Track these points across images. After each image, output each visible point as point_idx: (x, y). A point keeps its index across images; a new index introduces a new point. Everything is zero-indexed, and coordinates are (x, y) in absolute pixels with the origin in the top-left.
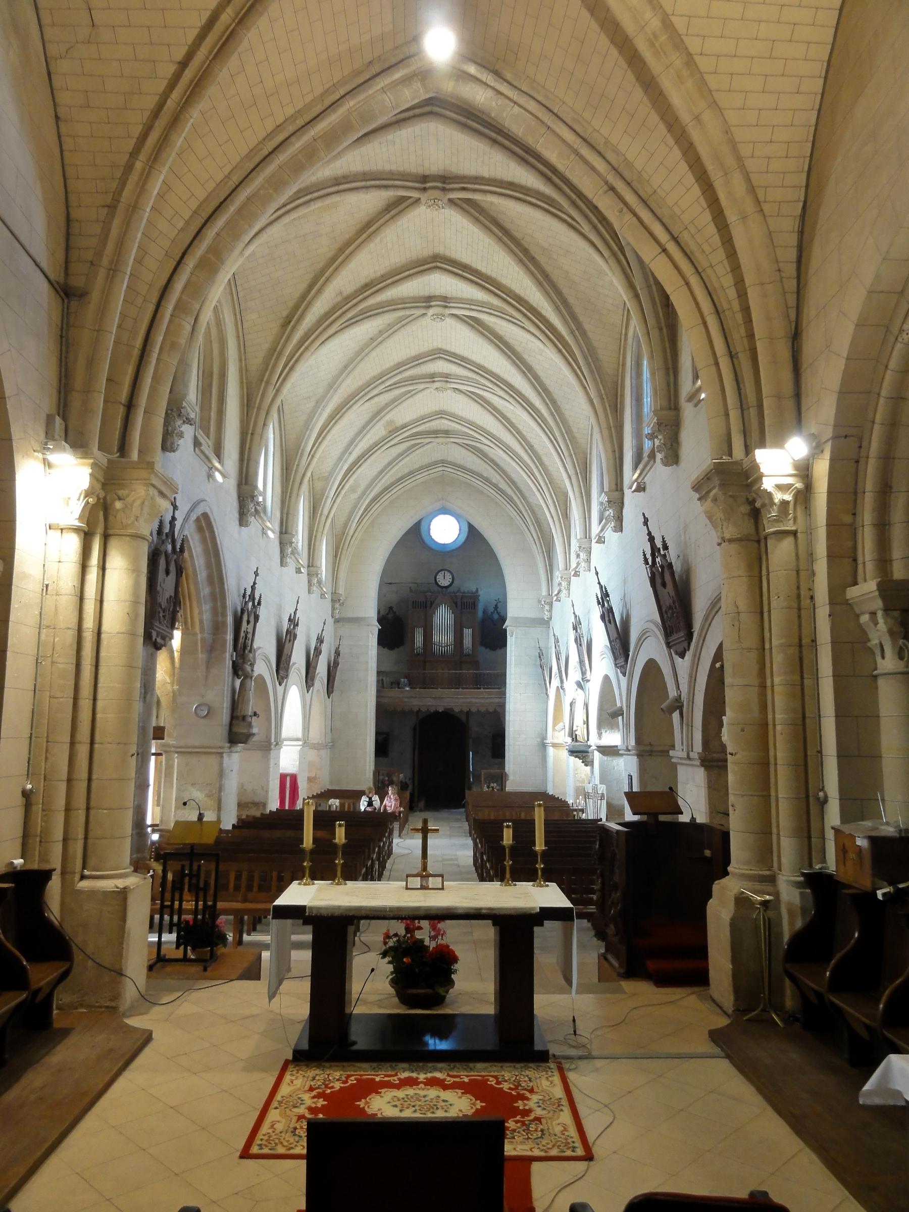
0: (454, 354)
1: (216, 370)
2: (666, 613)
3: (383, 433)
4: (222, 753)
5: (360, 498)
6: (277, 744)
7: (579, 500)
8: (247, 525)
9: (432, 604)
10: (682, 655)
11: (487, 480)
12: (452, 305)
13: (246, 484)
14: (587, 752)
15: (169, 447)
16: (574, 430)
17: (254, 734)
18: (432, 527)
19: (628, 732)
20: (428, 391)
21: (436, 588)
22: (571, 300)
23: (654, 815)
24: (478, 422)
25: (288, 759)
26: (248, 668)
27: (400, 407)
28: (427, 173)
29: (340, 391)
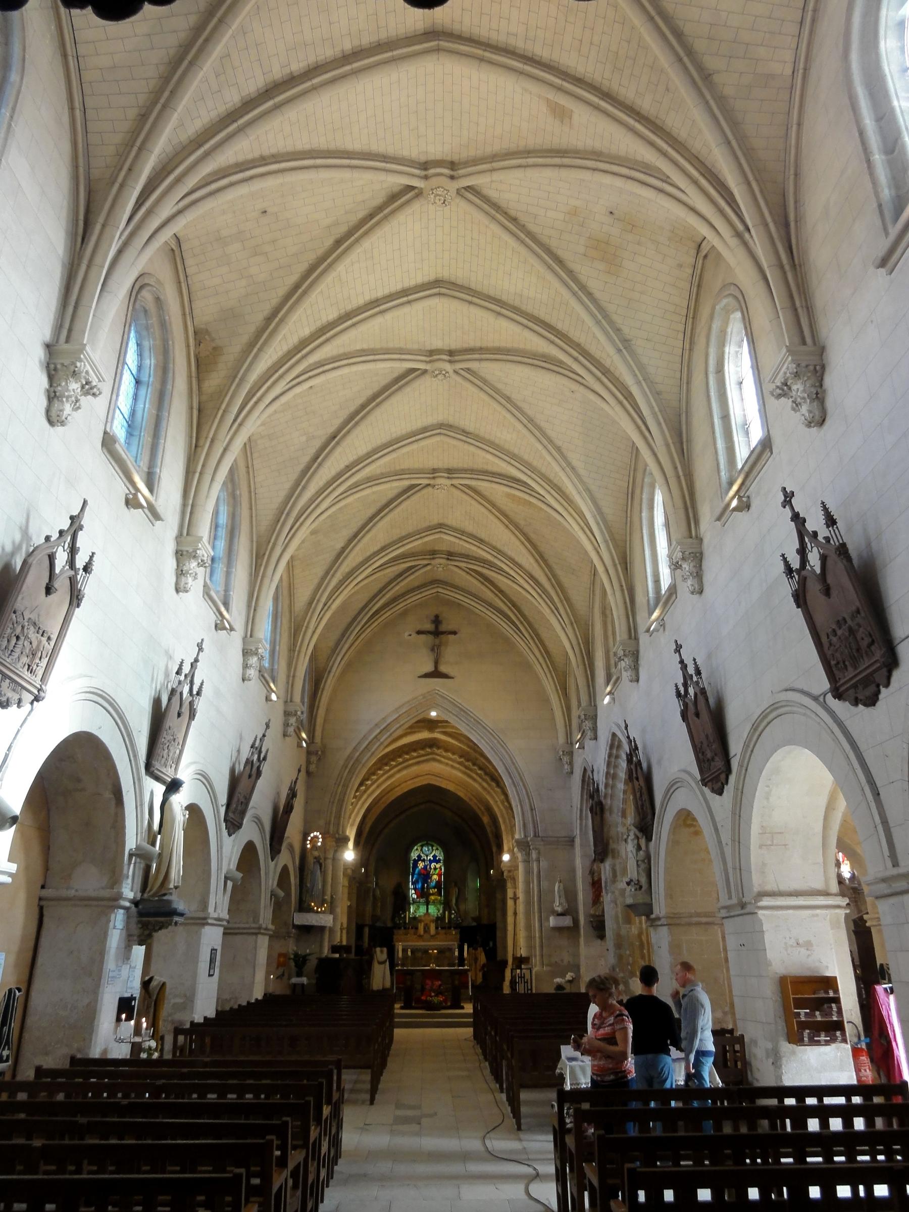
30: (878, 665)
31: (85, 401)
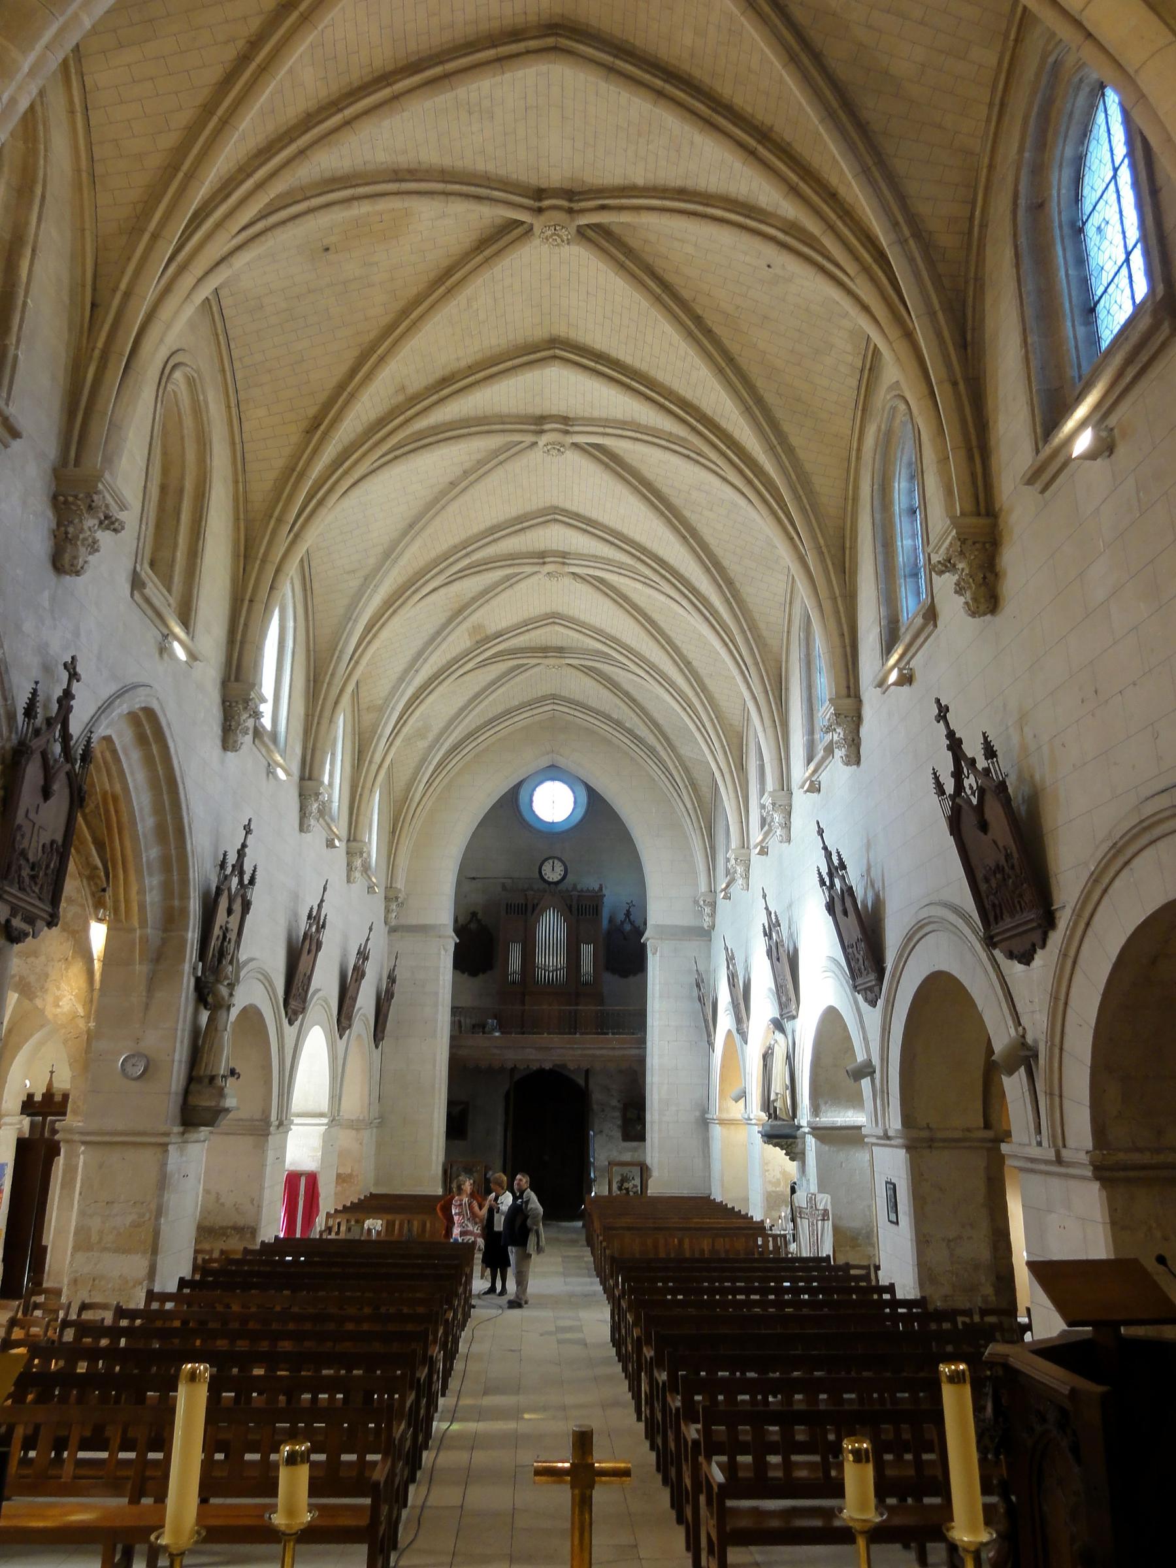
1: (189, 485)
2: (987, 880)
4: (166, 1145)
5: (431, 748)
6: (281, 1124)
7: (770, 731)
8: (235, 749)
9: (534, 907)
10: (1026, 958)
11: (618, 723)
13: (237, 679)
14: (795, 1137)
15: (67, 566)
16: (762, 626)
17: (227, 1110)
18: (535, 798)
19: (886, 1104)
20: (536, 577)
22: (770, 398)
24: (608, 630)
25: (302, 1147)
26: (224, 991)
27: (494, 602)
28: (544, 184)
29: (403, 562)
30: (1034, 924)
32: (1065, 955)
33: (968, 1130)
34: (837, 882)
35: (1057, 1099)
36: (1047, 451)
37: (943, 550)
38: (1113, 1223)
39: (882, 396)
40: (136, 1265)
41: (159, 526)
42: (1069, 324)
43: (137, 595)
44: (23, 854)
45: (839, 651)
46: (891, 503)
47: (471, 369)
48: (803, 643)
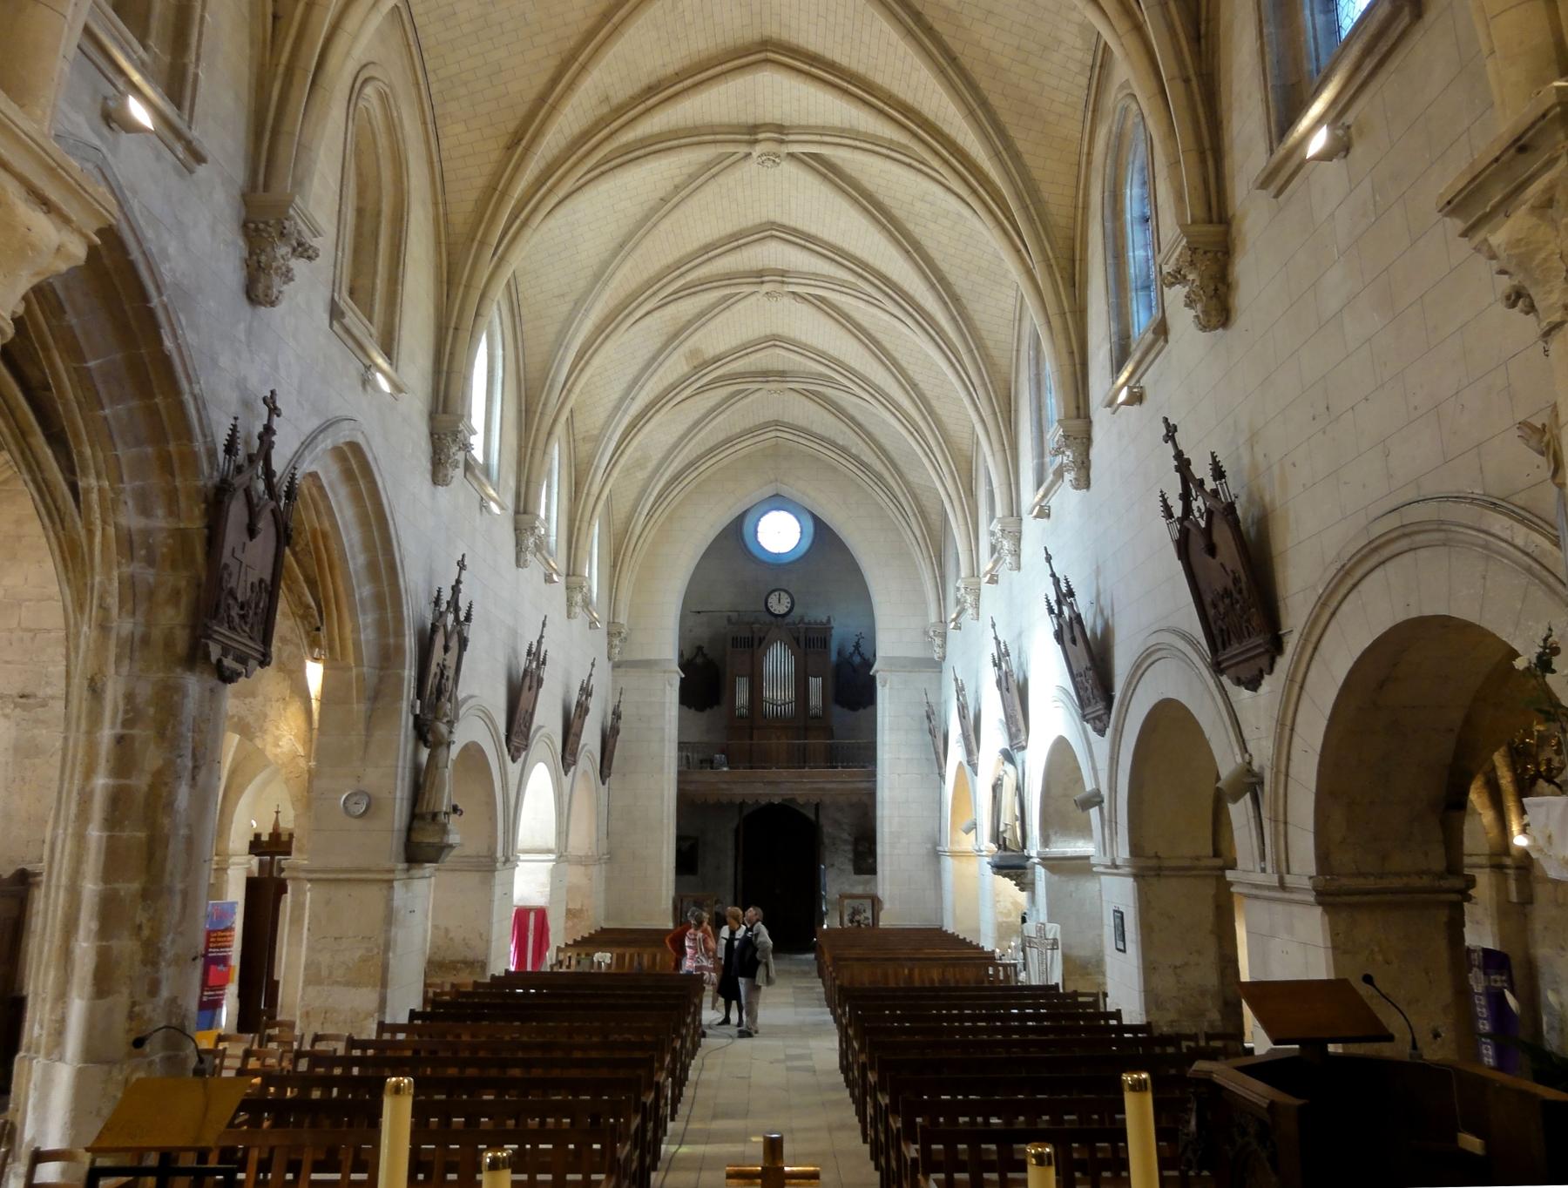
0: (795, 230)
1: (386, 208)
2: (1215, 606)
3: (685, 368)
4: (390, 881)
5: (651, 477)
6: (507, 860)
7: (999, 456)
9: (761, 640)
10: (1253, 684)
11: (844, 450)
12: (792, 137)
13: (445, 411)
16: (990, 344)
17: (451, 847)
19: (1114, 833)
20: (753, 299)
21: (768, 618)
22: (995, 100)
23: (1314, 1045)
24: (831, 352)
25: (530, 883)
26: (443, 728)
27: (711, 325)
29: (614, 283)
31: (298, 265)
32: (1292, 681)
33: (1198, 858)
34: (1065, 609)
35: (1281, 827)
36: (1281, 152)
37: (1173, 260)
38: (1335, 948)
39: (1113, 96)
40: (365, 998)
41: (357, 251)
42: (1307, 12)
43: (336, 325)
44: (232, 593)
45: (1068, 369)
46: (1122, 211)
47: (679, 76)
48: (1033, 363)
